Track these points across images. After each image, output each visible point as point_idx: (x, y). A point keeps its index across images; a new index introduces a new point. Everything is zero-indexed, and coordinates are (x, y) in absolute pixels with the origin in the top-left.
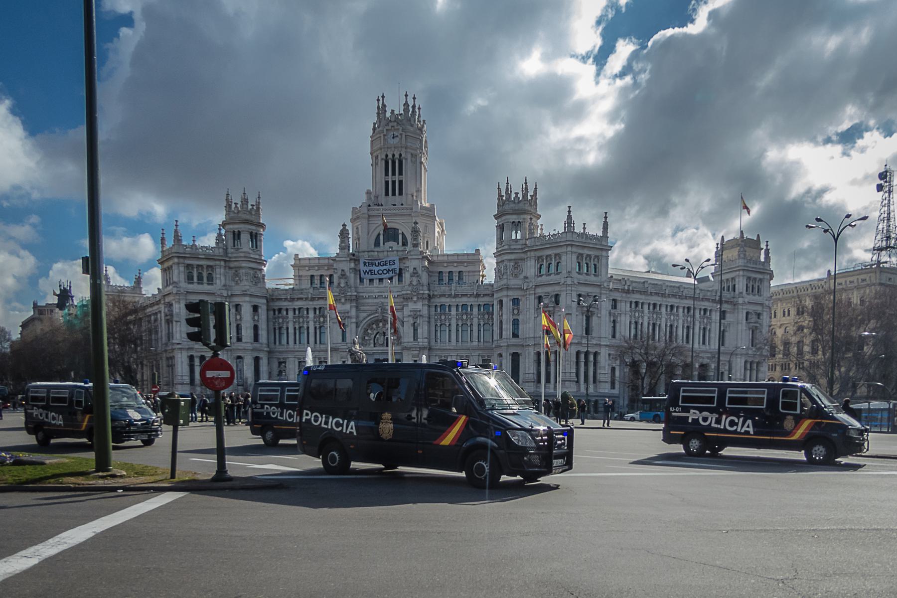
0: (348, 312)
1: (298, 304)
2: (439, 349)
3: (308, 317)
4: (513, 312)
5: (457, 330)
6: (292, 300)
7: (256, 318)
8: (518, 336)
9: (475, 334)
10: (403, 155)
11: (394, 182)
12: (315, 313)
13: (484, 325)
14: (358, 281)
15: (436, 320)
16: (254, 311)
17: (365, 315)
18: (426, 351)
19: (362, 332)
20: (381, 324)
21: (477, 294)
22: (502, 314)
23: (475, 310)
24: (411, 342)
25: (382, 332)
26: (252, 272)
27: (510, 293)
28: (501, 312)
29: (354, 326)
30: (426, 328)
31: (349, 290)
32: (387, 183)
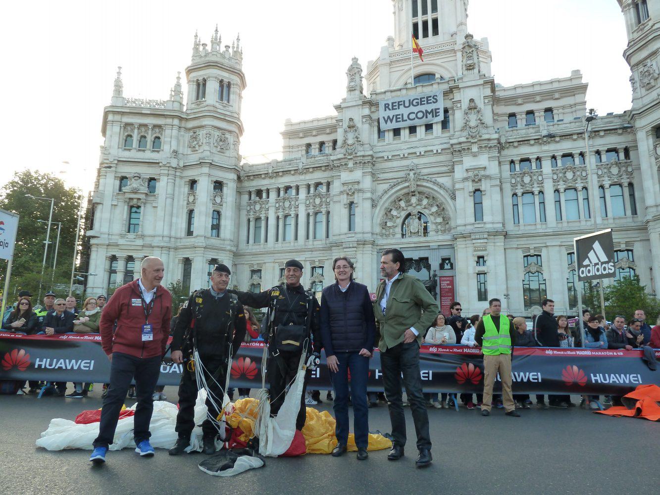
0: (359, 182)
2: (523, 236)
3: (297, 199)
6: (276, 174)
7: (218, 200)
11: (425, 23)
12: (309, 193)
14: (376, 136)
15: (514, 186)
17: (386, 186)
18: (500, 241)
19: (381, 215)
20: (414, 200)
24: (473, 224)
25: (415, 212)
26: (217, 133)
29: (368, 204)
30: (497, 196)
31: (362, 149)
32: (415, 26)
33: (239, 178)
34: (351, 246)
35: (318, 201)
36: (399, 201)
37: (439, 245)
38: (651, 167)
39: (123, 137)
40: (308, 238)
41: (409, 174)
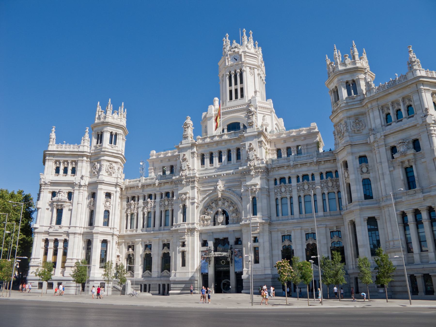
1: (148, 191)
4: (362, 171)
5: (300, 203)
8: (372, 198)
9: (320, 203)
10: (243, 69)
11: (236, 90)
13: (328, 193)
15: (276, 194)
16: (106, 198)
20: (220, 203)
21: (317, 162)
22: (348, 175)
23: (317, 178)
26: (108, 164)
27: (355, 149)
28: (346, 174)
30: (265, 201)
32: (231, 92)
33: (122, 189)
34: (183, 231)
35: (166, 203)
36: (212, 203)
37: (234, 230)
38: (344, 184)
39: (54, 167)
40: (161, 226)
41: (217, 188)
